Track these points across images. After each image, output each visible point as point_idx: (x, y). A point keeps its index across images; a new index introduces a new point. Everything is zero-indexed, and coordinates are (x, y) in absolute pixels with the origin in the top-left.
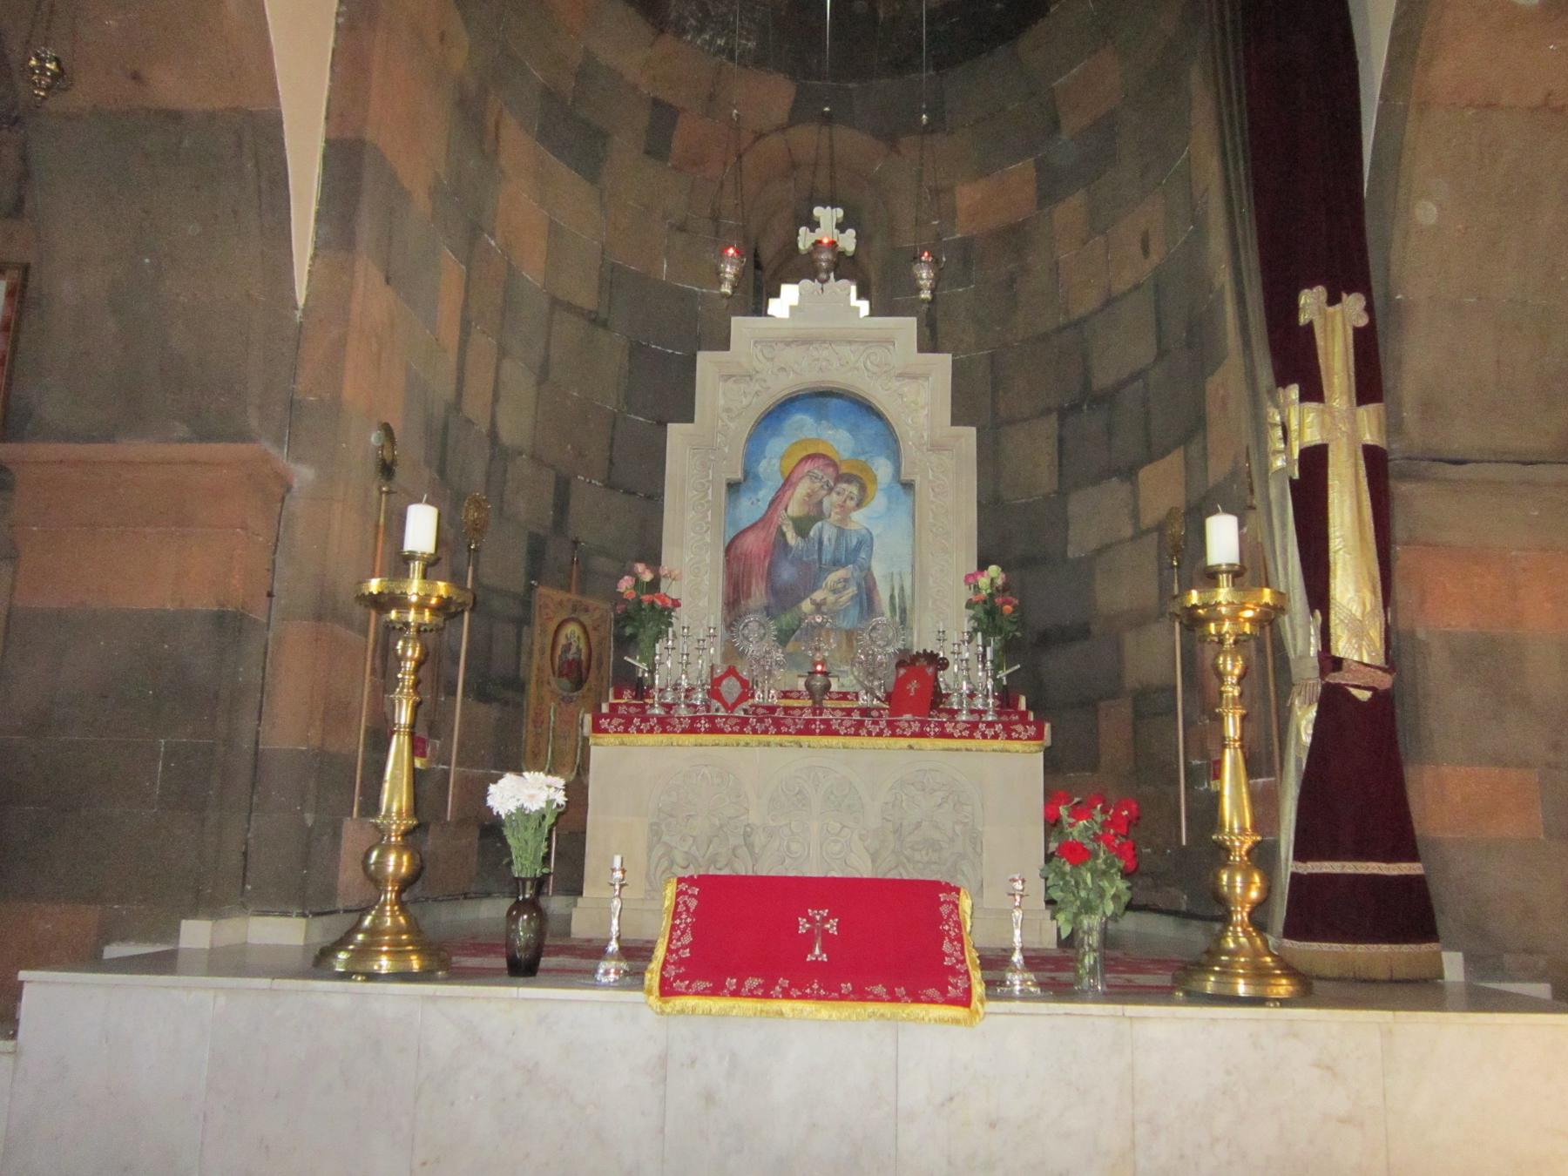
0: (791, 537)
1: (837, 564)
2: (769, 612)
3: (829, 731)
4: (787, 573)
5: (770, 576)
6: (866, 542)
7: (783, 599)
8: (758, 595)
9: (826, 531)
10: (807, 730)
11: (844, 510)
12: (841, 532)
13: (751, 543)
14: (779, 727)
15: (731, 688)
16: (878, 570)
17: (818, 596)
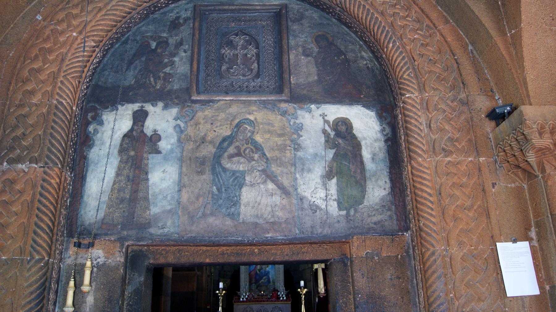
0: (258, 272)
1: (265, 276)
2: (255, 283)
3: (264, 301)
4: (258, 277)
5: (255, 278)
6: (269, 272)
7: (257, 281)
8: (253, 281)
9: (263, 271)
10: (261, 301)
11: (266, 268)
12: (265, 271)
13: (253, 273)
14: (258, 301)
15: (251, 296)
16: (270, 276)
17: (262, 281)
